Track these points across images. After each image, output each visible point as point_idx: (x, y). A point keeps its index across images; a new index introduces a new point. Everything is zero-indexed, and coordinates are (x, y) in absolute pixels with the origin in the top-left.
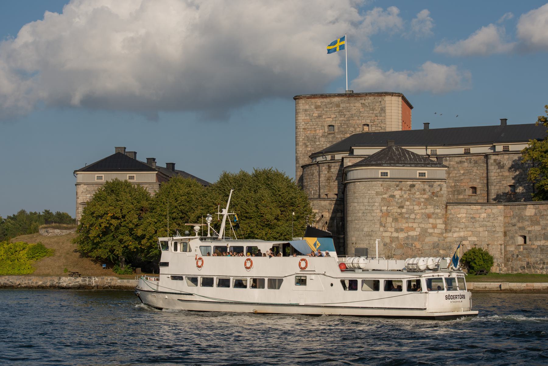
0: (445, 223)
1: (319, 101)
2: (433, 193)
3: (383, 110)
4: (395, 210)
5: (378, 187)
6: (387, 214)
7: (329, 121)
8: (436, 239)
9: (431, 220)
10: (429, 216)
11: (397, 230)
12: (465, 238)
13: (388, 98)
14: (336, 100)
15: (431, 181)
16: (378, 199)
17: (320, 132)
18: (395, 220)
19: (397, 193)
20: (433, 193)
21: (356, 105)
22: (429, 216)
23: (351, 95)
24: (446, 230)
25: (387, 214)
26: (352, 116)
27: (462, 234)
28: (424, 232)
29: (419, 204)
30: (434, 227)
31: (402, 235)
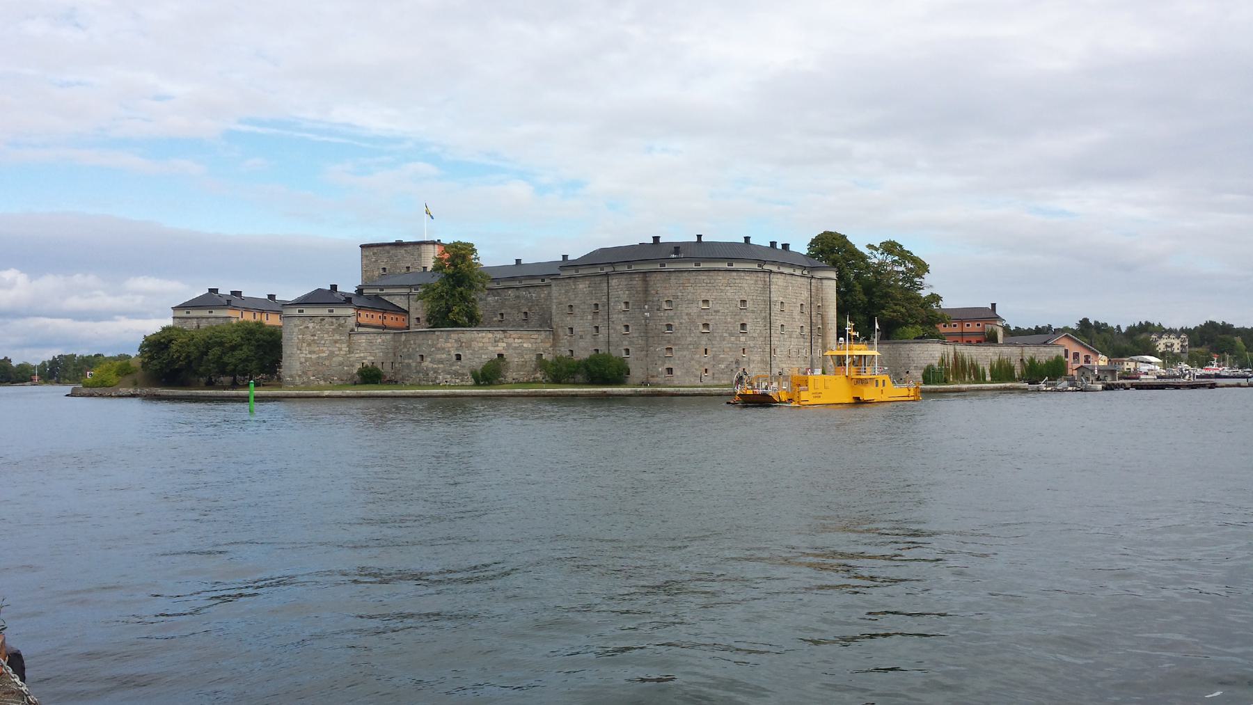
1: (375, 250)
3: (420, 255)
4: (309, 338)
5: (297, 322)
6: (303, 341)
10: (336, 342)
11: (310, 353)
12: (364, 358)
13: (424, 247)
14: (388, 248)
15: (338, 317)
16: (296, 330)
17: (376, 273)
18: (309, 345)
19: (311, 325)
21: (402, 251)
22: (336, 342)
23: (399, 244)
25: (303, 341)
28: (332, 353)
30: (340, 349)
31: (314, 356)
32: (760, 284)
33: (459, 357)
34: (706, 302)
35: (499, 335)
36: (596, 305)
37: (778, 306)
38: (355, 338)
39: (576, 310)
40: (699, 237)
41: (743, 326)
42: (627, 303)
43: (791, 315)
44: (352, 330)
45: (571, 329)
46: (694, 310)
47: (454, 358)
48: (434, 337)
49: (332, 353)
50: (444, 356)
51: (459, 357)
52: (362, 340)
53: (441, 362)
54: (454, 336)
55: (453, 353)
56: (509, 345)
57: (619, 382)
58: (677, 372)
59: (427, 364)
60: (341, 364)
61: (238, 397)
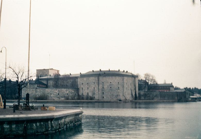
0: (36, 92)
2: (34, 87)
7: (41, 74)
8: (34, 94)
9: (33, 91)
10: (33, 90)
12: (39, 94)
20: (34, 87)
21: (45, 71)
23: (44, 69)
24: (36, 93)
26: (44, 73)
27: (38, 93)
28: (32, 93)
29: (31, 88)
30: (34, 92)
32: (122, 79)
33: (59, 94)
34: (111, 83)
35: (67, 89)
36: (88, 83)
37: (126, 84)
38: (37, 89)
39: (83, 84)
40: (109, 69)
41: (119, 88)
42: (94, 83)
43: (128, 85)
44: (36, 88)
45: (82, 88)
46: (108, 84)
47: (58, 94)
48: (54, 90)
49: (32, 93)
50: (56, 94)
51: (59, 94)
52: (38, 90)
53: (55, 95)
54: (58, 89)
55: (58, 93)
56: (69, 91)
57: (93, 100)
58: (105, 97)
59: (52, 95)
60: (34, 95)
61: (44, 102)
